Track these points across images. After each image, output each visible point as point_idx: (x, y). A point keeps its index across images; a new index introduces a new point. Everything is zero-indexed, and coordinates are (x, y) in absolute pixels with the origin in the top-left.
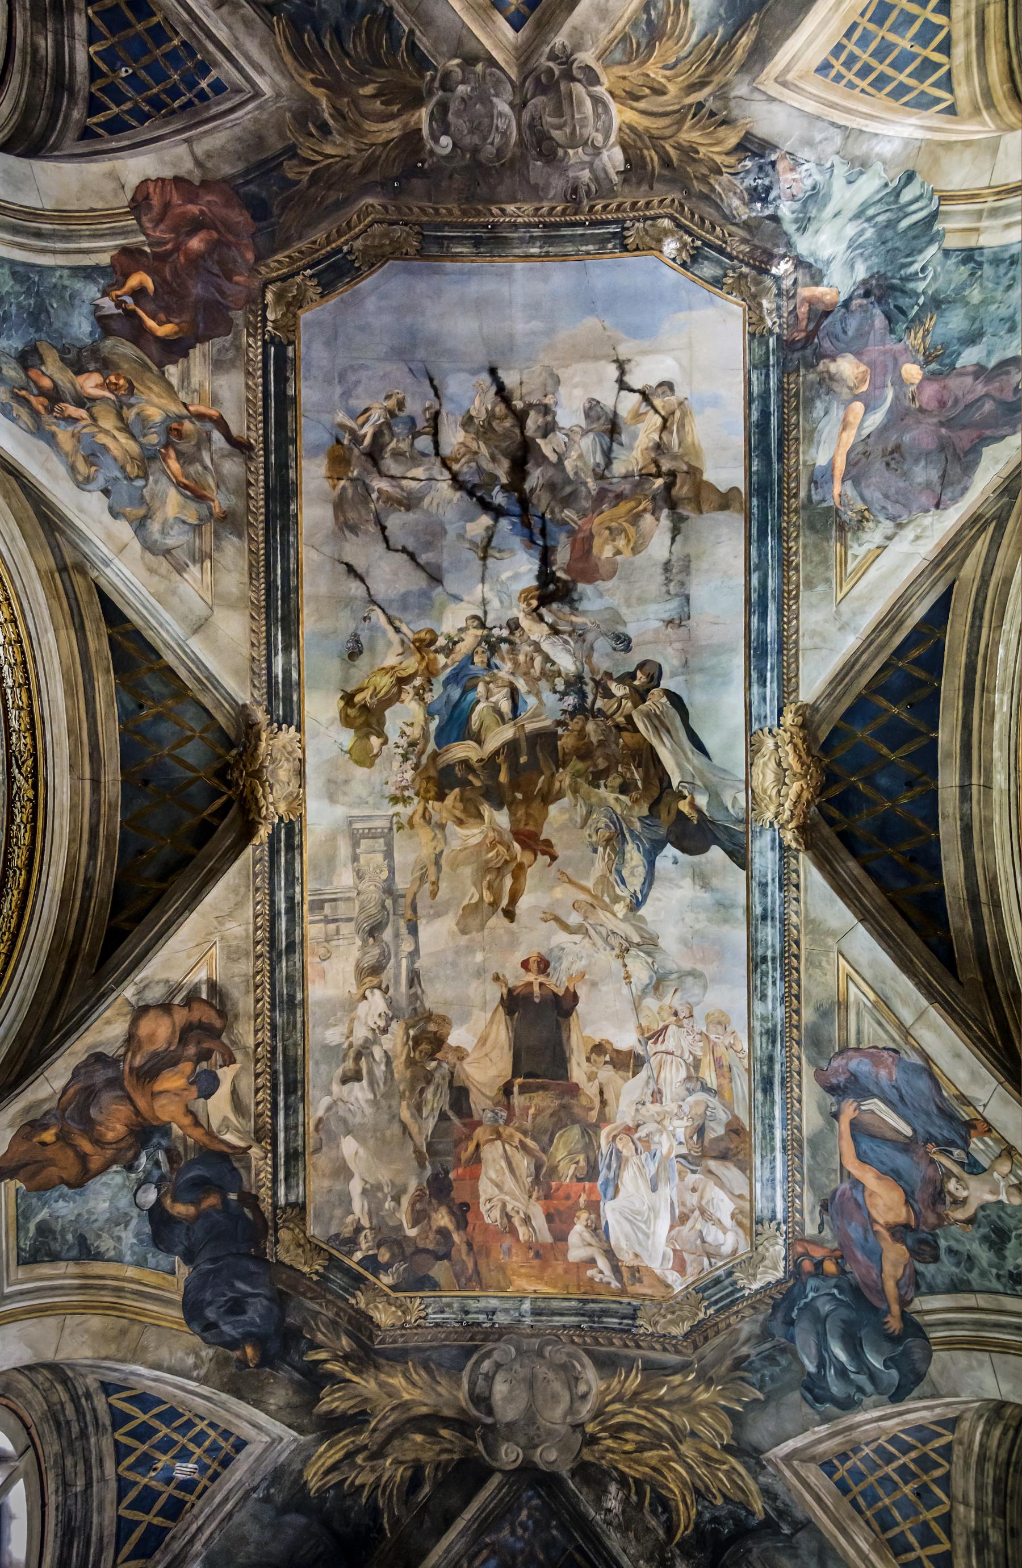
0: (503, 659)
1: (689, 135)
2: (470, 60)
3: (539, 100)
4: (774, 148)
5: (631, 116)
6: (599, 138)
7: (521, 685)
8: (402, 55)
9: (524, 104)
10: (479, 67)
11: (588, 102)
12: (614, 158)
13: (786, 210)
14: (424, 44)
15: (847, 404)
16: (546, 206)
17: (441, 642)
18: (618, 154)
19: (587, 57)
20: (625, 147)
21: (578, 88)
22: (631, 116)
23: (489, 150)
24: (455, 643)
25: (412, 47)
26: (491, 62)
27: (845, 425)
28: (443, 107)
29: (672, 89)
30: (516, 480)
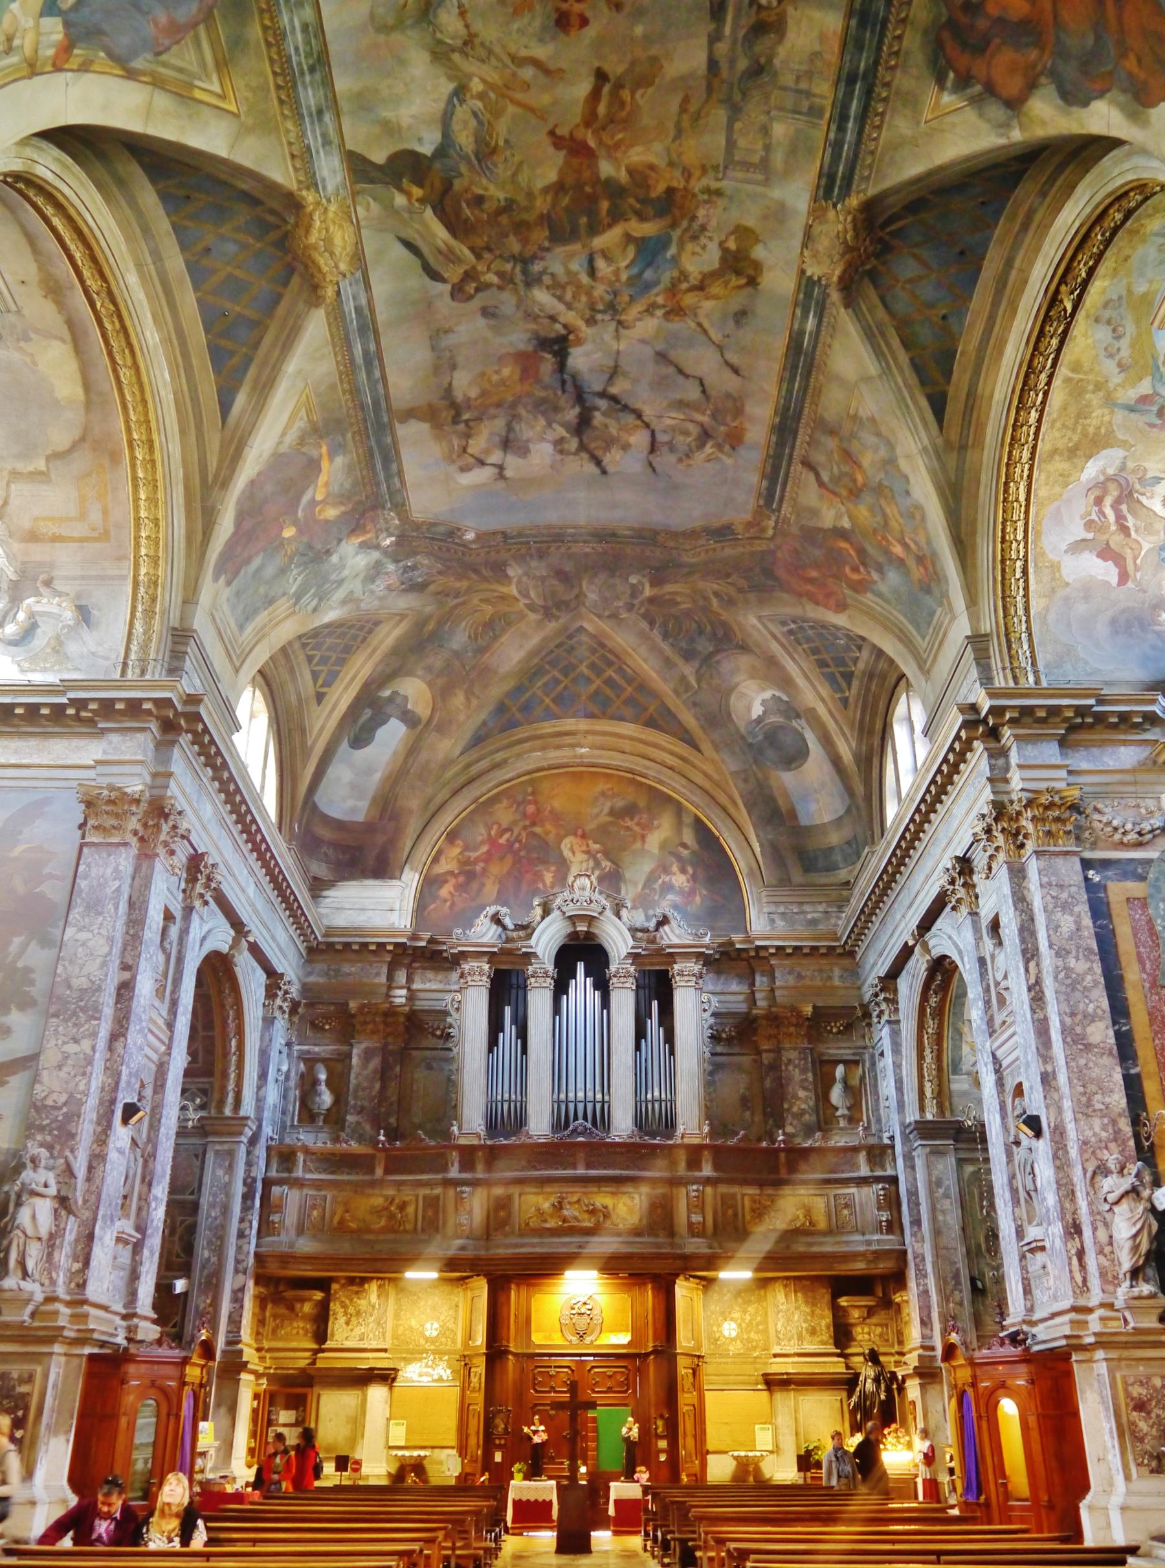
0: (602, 298)
1: (465, 584)
2: (614, 616)
3: (566, 598)
4: (403, 590)
5: (504, 590)
6: (525, 579)
7: (585, 279)
8: (659, 621)
9: (577, 597)
10: (607, 613)
11: (532, 594)
12: (514, 571)
13: (391, 567)
14: (644, 625)
15: (328, 495)
16: (562, 550)
17: (659, 313)
18: (511, 572)
19: (533, 617)
20: (507, 576)
21: (540, 602)
22: (504, 590)
23: (602, 577)
24: (647, 310)
25: (652, 623)
26: (599, 616)
27: (327, 484)
28: (634, 595)
29: (476, 601)
30: (588, 416)
